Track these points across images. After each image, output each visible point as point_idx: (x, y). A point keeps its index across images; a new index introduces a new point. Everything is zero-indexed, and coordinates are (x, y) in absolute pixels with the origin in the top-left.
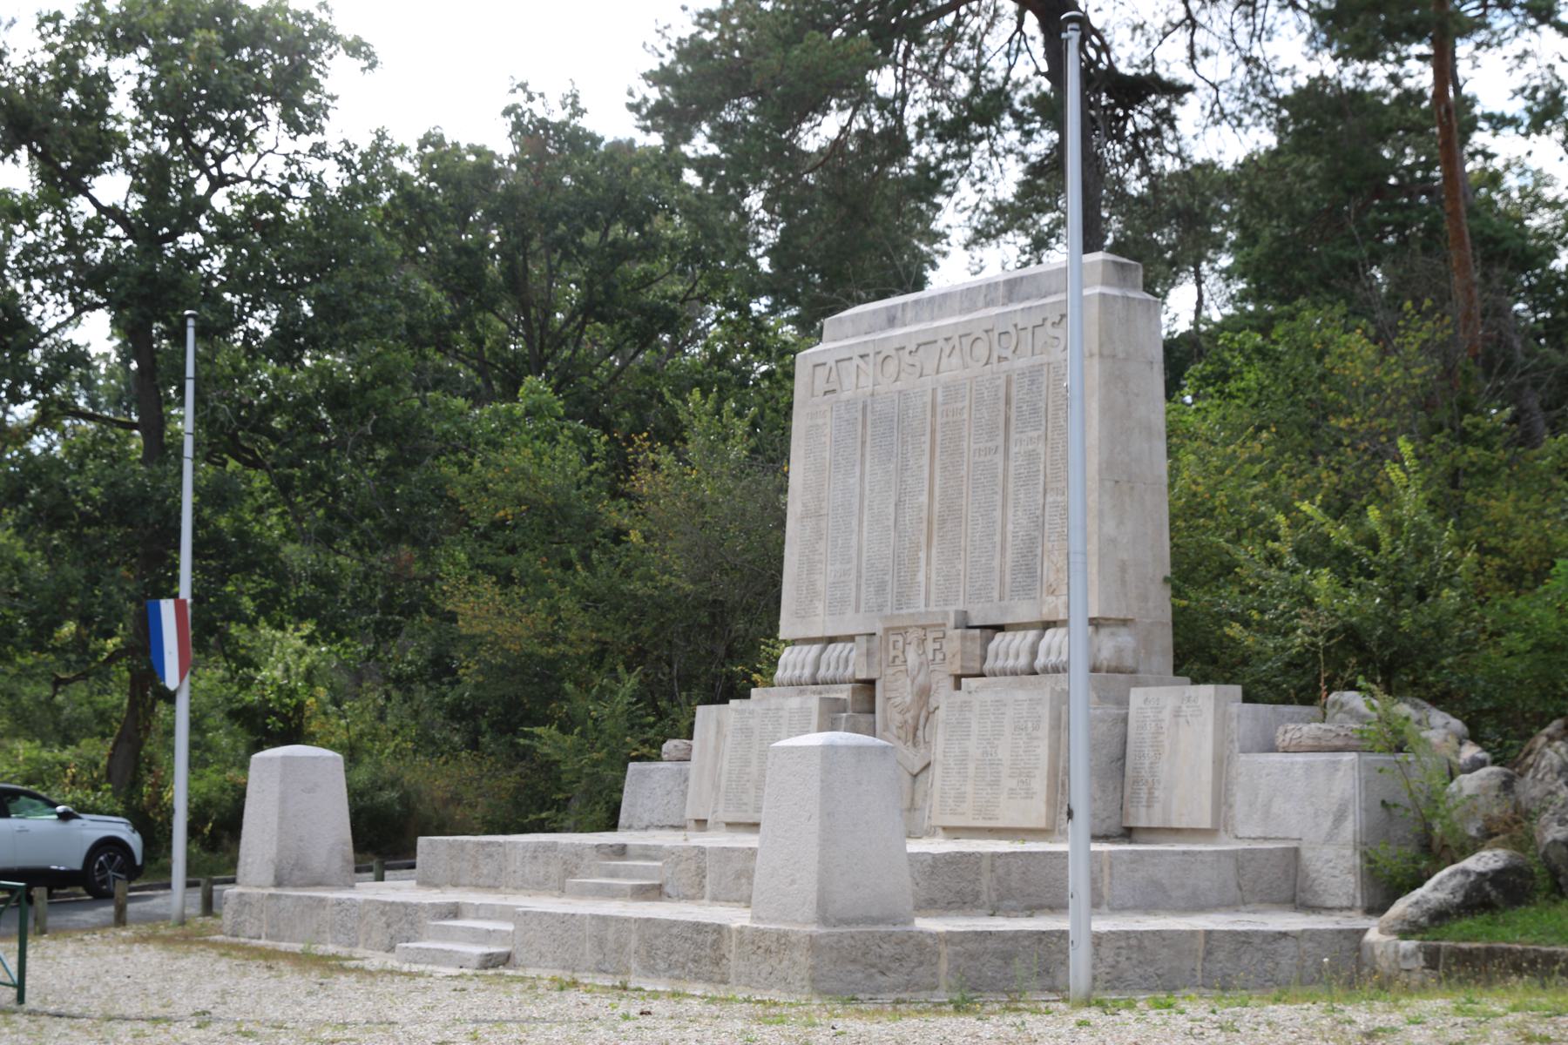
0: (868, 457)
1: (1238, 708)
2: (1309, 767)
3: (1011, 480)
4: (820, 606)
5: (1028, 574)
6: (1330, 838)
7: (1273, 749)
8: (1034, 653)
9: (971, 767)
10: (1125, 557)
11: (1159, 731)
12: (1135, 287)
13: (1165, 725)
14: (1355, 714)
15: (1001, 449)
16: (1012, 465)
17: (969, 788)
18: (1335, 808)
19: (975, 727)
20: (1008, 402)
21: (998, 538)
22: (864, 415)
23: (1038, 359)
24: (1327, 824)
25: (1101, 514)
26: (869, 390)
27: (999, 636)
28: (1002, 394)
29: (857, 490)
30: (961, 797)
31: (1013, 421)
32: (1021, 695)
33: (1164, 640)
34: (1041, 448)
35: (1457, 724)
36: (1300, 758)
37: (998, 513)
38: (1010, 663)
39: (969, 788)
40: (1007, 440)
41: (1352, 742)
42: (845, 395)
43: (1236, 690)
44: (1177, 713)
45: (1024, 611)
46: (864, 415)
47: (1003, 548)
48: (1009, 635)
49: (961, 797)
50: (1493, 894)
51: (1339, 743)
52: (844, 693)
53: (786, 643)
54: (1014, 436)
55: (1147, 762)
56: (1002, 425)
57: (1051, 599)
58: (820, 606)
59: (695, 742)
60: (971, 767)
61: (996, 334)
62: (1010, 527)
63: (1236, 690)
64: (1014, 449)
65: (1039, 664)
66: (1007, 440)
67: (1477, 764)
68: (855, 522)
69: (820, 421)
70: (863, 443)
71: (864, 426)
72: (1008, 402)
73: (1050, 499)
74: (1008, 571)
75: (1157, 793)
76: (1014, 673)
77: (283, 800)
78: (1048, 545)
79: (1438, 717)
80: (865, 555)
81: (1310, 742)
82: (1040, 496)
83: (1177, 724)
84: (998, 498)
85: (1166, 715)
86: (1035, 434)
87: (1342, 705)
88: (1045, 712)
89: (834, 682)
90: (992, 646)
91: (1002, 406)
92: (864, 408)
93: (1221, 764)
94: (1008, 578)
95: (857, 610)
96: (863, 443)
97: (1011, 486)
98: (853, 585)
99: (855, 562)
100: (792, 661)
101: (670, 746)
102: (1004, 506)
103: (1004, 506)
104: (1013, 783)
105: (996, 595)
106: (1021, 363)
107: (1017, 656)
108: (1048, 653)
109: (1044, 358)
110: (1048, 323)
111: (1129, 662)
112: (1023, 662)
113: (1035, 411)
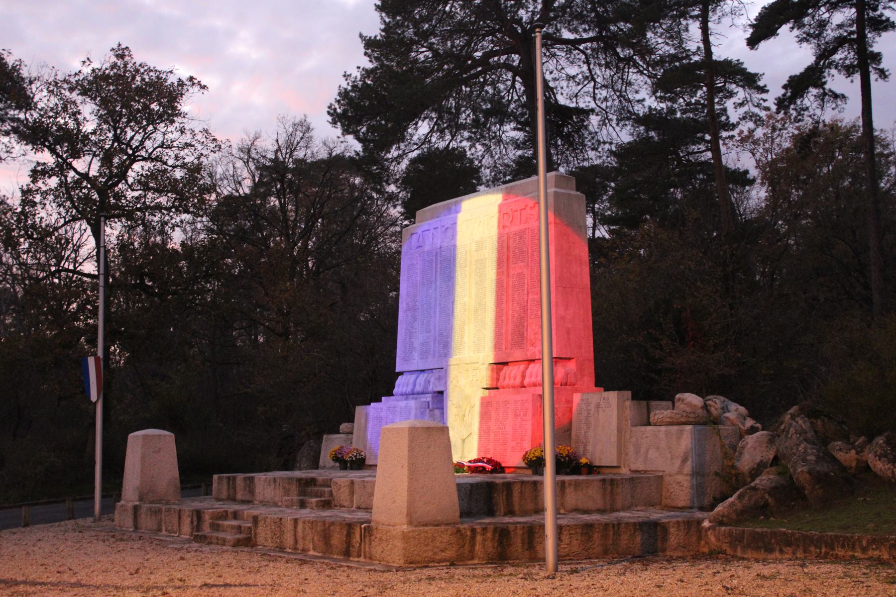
0: (438, 279)
1: (628, 403)
2: (667, 434)
3: (510, 288)
6: (680, 472)
7: (649, 424)
8: (523, 377)
10: (570, 326)
11: (588, 417)
12: (571, 189)
13: (592, 412)
14: (689, 404)
15: (505, 273)
18: (682, 454)
19: (493, 415)
20: (508, 248)
21: (504, 318)
22: (436, 258)
23: (523, 227)
24: (678, 463)
25: (557, 305)
27: (506, 368)
32: (518, 397)
33: (590, 368)
34: (525, 271)
35: (742, 409)
36: (663, 428)
40: (508, 269)
41: (691, 420)
42: (427, 248)
43: (628, 394)
44: (598, 406)
45: (518, 355)
46: (436, 258)
47: (507, 323)
50: (770, 500)
51: (683, 420)
52: (428, 398)
53: (401, 373)
54: (512, 266)
55: (583, 432)
57: (531, 348)
58: (416, 355)
59: (355, 424)
60: (492, 435)
62: (510, 312)
63: (628, 394)
64: (512, 272)
65: (526, 382)
66: (508, 269)
67: (752, 430)
70: (436, 272)
71: (436, 264)
72: (508, 248)
73: (531, 297)
74: (510, 335)
75: (588, 448)
76: (514, 387)
77: (143, 457)
78: (530, 321)
79: (733, 406)
81: (668, 420)
82: (525, 296)
83: (598, 411)
85: (592, 407)
86: (522, 264)
87: (683, 400)
88: (529, 406)
89: (423, 393)
90: (502, 373)
91: (505, 250)
93: (620, 431)
94: (510, 338)
96: (436, 272)
97: (510, 292)
98: (432, 344)
100: (402, 384)
101: (344, 427)
102: (507, 302)
103: (507, 302)
104: (514, 444)
105: (504, 347)
107: (515, 379)
108: (531, 376)
109: (526, 226)
110: (528, 208)
111: (572, 379)
112: (518, 381)
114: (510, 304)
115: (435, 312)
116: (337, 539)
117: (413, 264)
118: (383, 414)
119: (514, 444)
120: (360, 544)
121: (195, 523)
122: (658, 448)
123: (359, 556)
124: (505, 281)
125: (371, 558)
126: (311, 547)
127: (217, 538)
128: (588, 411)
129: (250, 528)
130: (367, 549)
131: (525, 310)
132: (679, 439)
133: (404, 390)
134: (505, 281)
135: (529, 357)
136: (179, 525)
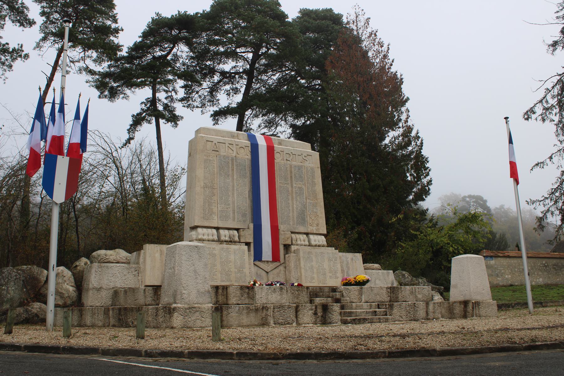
2: (383, 273)
3: (294, 193)
4: (216, 217)
5: (302, 219)
9: (315, 271)
13: (349, 262)
15: (290, 184)
16: (294, 189)
17: (315, 276)
19: (314, 259)
20: (291, 172)
21: (291, 208)
26: (234, 154)
28: (288, 169)
29: (231, 184)
30: (313, 278)
31: (293, 177)
37: (290, 202)
38: (303, 243)
39: (315, 276)
42: (223, 152)
44: (352, 259)
45: (302, 229)
47: (293, 212)
48: (298, 236)
49: (313, 278)
54: (294, 182)
56: (289, 178)
60: (315, 271)
61: (285, 153)
62: (295, 206)
68: (230, 193)
69: (211, 159)
70: (233, 170)
71: (233, 165)
72: (291, 172)
73: (308, 201)
80: (236, 204)
82: (305, 200)
84: (290, 197)
85: (349, 260)
91: (289, 172)
92: (232, 159)
95: (234, 220)
97: (294, 195)
99: (231, 206)
104: (331, 275)
105: (291, 223)
106: (294, 163)
109: (303, 164)
113: (301, 177)
114: (295, 202)
115: (233, 194)
116: (458, 309)
117: (210, 160)
118: (216, 252)
119: (331, 275)
120: (473, 311)
121: (320, 314)
122: (380, 280)
123: (473, 316)
124: (290, 189)
125: (480, 316)
126: (440, 316)
127: (380, 318)
128: (347, 262)
129: (386, 311)
130: (477, 312)
131: (305, 206)
132: (388, 276)
133: (211, 238)
134: (290, 189)
135: (309, 231)
136: (297, 317)
